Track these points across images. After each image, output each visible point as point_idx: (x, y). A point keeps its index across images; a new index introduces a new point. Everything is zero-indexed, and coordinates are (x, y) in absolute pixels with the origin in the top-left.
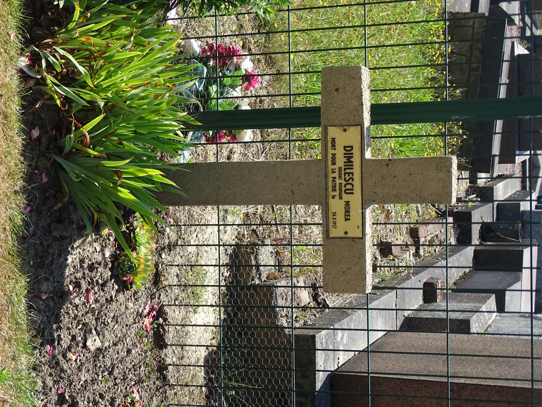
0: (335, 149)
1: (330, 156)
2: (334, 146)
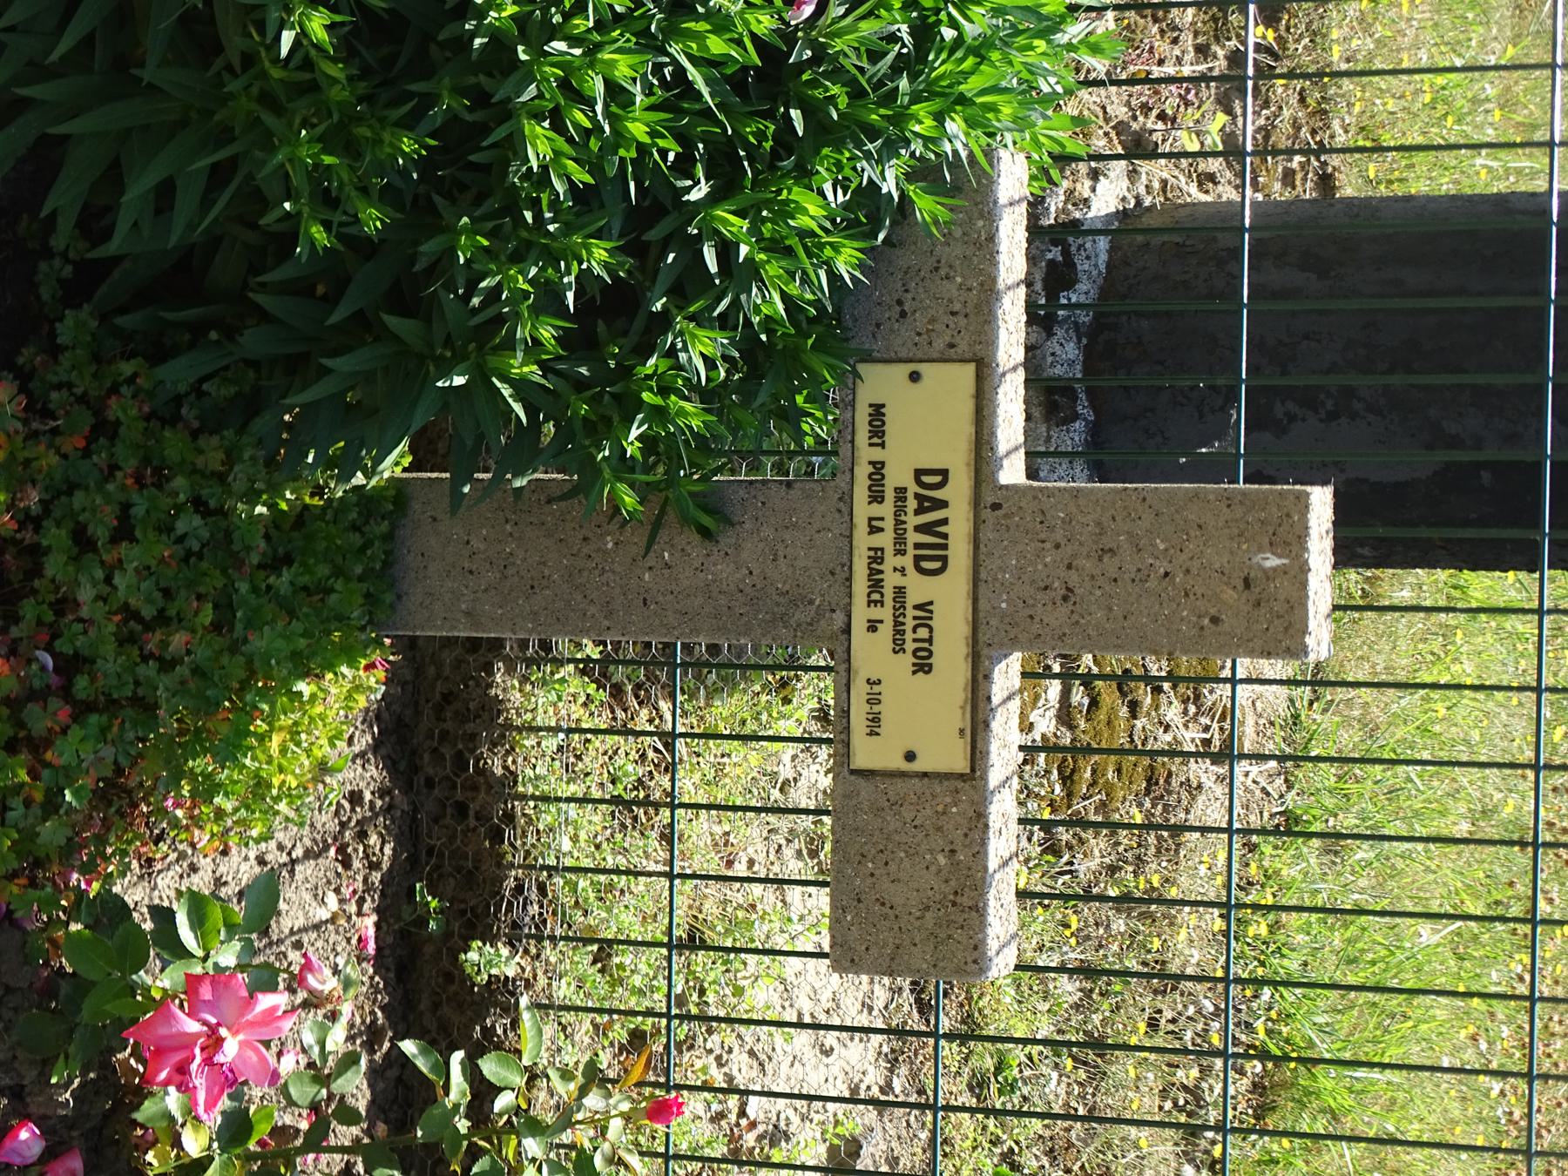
0: (883, 445)
1: (863, 472)
2: (878, 433)
